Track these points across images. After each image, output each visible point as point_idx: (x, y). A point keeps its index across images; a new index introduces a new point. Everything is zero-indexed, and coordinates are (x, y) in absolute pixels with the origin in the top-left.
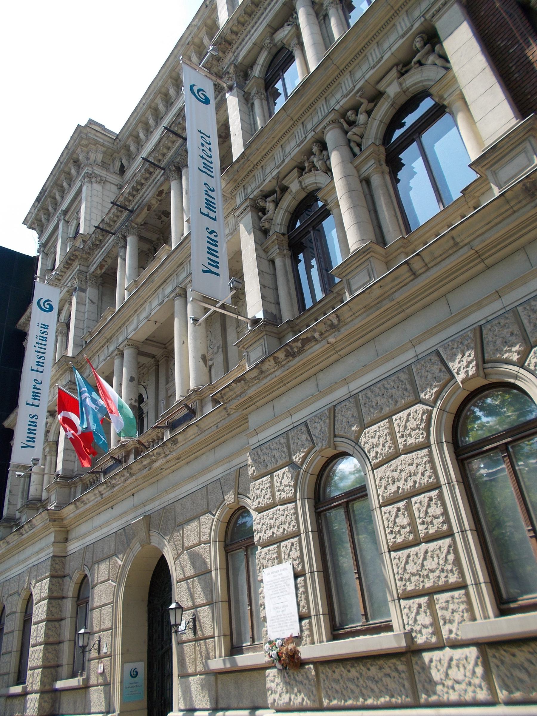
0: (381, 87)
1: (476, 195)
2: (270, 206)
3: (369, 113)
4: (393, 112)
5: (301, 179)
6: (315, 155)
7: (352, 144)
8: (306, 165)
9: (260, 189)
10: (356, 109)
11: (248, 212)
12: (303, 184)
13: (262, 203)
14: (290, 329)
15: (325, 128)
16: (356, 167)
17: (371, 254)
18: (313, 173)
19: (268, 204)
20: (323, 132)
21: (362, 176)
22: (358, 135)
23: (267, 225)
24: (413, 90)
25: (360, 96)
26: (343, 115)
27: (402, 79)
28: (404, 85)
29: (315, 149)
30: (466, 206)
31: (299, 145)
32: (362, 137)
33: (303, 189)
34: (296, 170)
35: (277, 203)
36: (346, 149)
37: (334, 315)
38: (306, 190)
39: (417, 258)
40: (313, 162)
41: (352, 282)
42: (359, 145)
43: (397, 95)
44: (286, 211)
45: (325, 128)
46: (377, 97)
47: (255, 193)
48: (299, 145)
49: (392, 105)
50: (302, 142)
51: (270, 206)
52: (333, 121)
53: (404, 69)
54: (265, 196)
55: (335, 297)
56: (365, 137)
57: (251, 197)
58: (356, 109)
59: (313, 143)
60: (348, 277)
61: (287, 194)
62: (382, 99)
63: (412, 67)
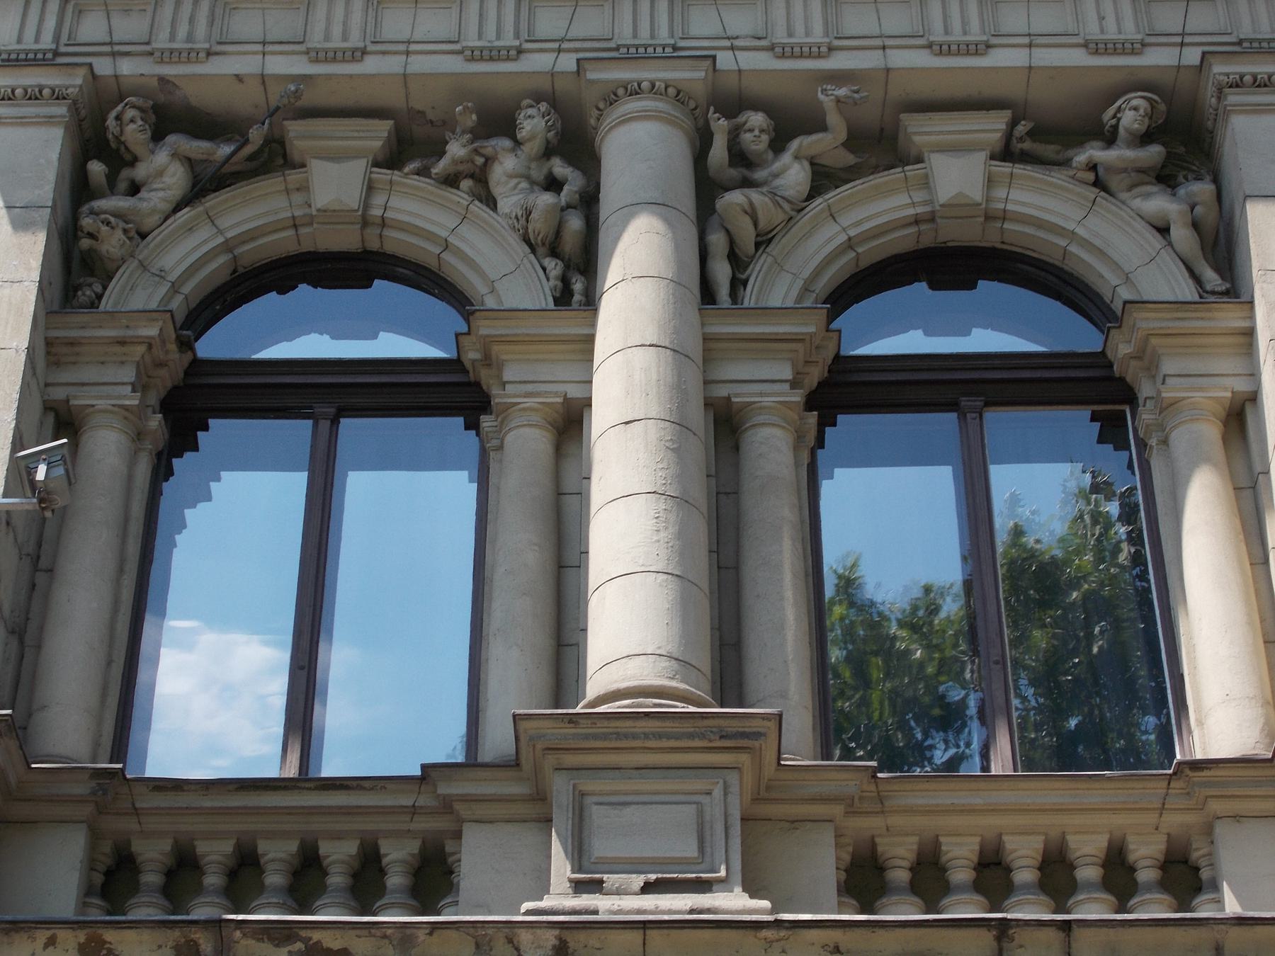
0: (923, 130)
1: (1216, 807)
2: (164, 171)
3: (824, 178)
4: (902, 241)
5: (383, 175)
6: (518, 143)
7: (717, 240)
8: (456, 149)
9: (168, 70)
10: (789, 124)
11: (49, 121)
12: (379, 199)
13: (134, 133)
14: (88, 810)
15: (634, 91)
16: (706, 339)
17: (744, 758)
18: (460, 197)
19: (162, 157)
20: (612, 97)
21: (722, 391)
22: (756, 224)
23: (112, 243)
24: (1017, 235)
25: (838, 101)
26: (732, 103)
27: (1006, 168)
28: (1000, 193)
29: (533, 124)
30: (1152, 818)
31: (474, 55)
32: (764, 241)
33: (365, 222)
34: (383, 128)
35: (205, 184)
36: (692, 233)
37: (550, 938)
38: (372, 233)
39: (1053, 935)
40: (489, 161)
41: (598, 815)
42: (734, 258)
43: (960, 209)
44: (227, 247)
45: (634, 91)
46: (880, 145)
47: (127, 67)
48: (474, 55)
49: (917, 221)
50: (492, 55)
51: (164, 171)
52: (679, 96)
53: (1027, 145)
54: (168, 118)
55: (414, 811)
56: (774, 249)
57: (103, 67)
58: (789, 124)
59: (538, 98)
60: (588, 785)
61: (269, 185)
62: (896, 174)
63: (1065, 163)
